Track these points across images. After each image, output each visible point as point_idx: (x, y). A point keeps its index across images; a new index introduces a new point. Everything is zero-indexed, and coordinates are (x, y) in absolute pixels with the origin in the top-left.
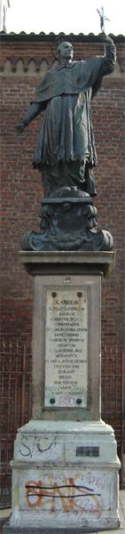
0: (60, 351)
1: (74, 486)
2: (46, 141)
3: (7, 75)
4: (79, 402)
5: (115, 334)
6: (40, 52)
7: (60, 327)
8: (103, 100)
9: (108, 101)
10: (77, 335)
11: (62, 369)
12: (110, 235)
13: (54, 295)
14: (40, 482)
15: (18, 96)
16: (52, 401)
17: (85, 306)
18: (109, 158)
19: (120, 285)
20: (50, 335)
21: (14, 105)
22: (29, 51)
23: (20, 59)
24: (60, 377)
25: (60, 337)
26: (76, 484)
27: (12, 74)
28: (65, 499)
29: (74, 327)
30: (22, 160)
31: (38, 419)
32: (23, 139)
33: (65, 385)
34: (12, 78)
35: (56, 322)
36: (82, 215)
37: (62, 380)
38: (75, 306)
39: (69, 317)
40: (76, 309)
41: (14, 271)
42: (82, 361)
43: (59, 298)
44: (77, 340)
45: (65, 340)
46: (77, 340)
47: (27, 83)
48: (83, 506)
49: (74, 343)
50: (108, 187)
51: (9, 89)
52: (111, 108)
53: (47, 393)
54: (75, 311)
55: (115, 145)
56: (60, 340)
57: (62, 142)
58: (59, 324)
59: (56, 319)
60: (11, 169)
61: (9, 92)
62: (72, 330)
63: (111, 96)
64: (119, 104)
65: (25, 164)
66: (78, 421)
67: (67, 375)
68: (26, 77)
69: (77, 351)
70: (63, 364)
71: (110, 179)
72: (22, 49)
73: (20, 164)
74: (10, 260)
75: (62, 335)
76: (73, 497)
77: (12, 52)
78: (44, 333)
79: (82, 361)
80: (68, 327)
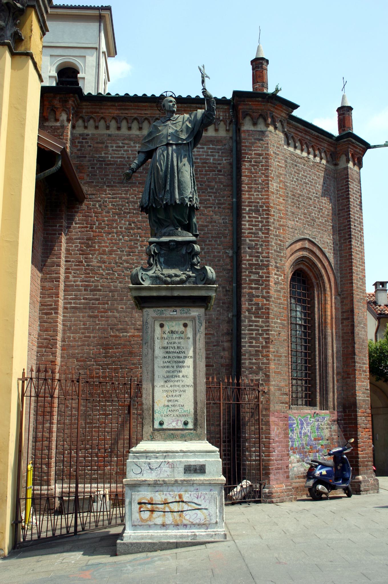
0: (167, 377)
1: (183, 502)
2: (152, 186)
3: (113, 133)
4: (186, 423)
5: (212, 366)
6: (143, 112)
7: (167, 355)
8: (200, 155)
9: (204, 157)
11: (171, 394)
12: (213, 270)
13: (162, 326)
14: (151, 499)
15: (122, 152)
16: (161, 424)
17: (190, 335)
18: (205, 207)
19: (216, 322)
20: (159, 363)
21: (119, 160)
22: (133, 111)
23: (125, 118)
25: (168, 364)
26: (185, 500)
27: (117, 132)
28: (175, 514)
29: (180, 355)
30: (127, 209)
31: (148, 440)
33: (173, 408)
34: (117, 136)
35: (164, 350)
36: (186, 252)
39: (176, 345)
40: (182, 338)
43: (166, 328)
45: (173, 367)
47: (131, 140)
48: (191, 520)
50: (204, 234)
51: (114, 145)
52: (206, 163)
53: (156, 416)
54: (181, 340)
55: (211, 196)
56: (168, 367)
57: (168, 188)
58: (167, 352)
59: (164, 348)
60: (117, 217)
61: (114, 148)
62: (178, 357)
63: (208, 152)
64: (214, 159)
65: (129, 213)
66: (186, 441)
67: (176, 398)
68: (130, 135)
69: (183, 376)
70: (171, 389)
71: (207, 226)
72: (128, 109)
73: (125, 213)
74: (116, 300)
76: (182, 511)
77: (117, 112)
78: (153, 360)
80: (176, 355)
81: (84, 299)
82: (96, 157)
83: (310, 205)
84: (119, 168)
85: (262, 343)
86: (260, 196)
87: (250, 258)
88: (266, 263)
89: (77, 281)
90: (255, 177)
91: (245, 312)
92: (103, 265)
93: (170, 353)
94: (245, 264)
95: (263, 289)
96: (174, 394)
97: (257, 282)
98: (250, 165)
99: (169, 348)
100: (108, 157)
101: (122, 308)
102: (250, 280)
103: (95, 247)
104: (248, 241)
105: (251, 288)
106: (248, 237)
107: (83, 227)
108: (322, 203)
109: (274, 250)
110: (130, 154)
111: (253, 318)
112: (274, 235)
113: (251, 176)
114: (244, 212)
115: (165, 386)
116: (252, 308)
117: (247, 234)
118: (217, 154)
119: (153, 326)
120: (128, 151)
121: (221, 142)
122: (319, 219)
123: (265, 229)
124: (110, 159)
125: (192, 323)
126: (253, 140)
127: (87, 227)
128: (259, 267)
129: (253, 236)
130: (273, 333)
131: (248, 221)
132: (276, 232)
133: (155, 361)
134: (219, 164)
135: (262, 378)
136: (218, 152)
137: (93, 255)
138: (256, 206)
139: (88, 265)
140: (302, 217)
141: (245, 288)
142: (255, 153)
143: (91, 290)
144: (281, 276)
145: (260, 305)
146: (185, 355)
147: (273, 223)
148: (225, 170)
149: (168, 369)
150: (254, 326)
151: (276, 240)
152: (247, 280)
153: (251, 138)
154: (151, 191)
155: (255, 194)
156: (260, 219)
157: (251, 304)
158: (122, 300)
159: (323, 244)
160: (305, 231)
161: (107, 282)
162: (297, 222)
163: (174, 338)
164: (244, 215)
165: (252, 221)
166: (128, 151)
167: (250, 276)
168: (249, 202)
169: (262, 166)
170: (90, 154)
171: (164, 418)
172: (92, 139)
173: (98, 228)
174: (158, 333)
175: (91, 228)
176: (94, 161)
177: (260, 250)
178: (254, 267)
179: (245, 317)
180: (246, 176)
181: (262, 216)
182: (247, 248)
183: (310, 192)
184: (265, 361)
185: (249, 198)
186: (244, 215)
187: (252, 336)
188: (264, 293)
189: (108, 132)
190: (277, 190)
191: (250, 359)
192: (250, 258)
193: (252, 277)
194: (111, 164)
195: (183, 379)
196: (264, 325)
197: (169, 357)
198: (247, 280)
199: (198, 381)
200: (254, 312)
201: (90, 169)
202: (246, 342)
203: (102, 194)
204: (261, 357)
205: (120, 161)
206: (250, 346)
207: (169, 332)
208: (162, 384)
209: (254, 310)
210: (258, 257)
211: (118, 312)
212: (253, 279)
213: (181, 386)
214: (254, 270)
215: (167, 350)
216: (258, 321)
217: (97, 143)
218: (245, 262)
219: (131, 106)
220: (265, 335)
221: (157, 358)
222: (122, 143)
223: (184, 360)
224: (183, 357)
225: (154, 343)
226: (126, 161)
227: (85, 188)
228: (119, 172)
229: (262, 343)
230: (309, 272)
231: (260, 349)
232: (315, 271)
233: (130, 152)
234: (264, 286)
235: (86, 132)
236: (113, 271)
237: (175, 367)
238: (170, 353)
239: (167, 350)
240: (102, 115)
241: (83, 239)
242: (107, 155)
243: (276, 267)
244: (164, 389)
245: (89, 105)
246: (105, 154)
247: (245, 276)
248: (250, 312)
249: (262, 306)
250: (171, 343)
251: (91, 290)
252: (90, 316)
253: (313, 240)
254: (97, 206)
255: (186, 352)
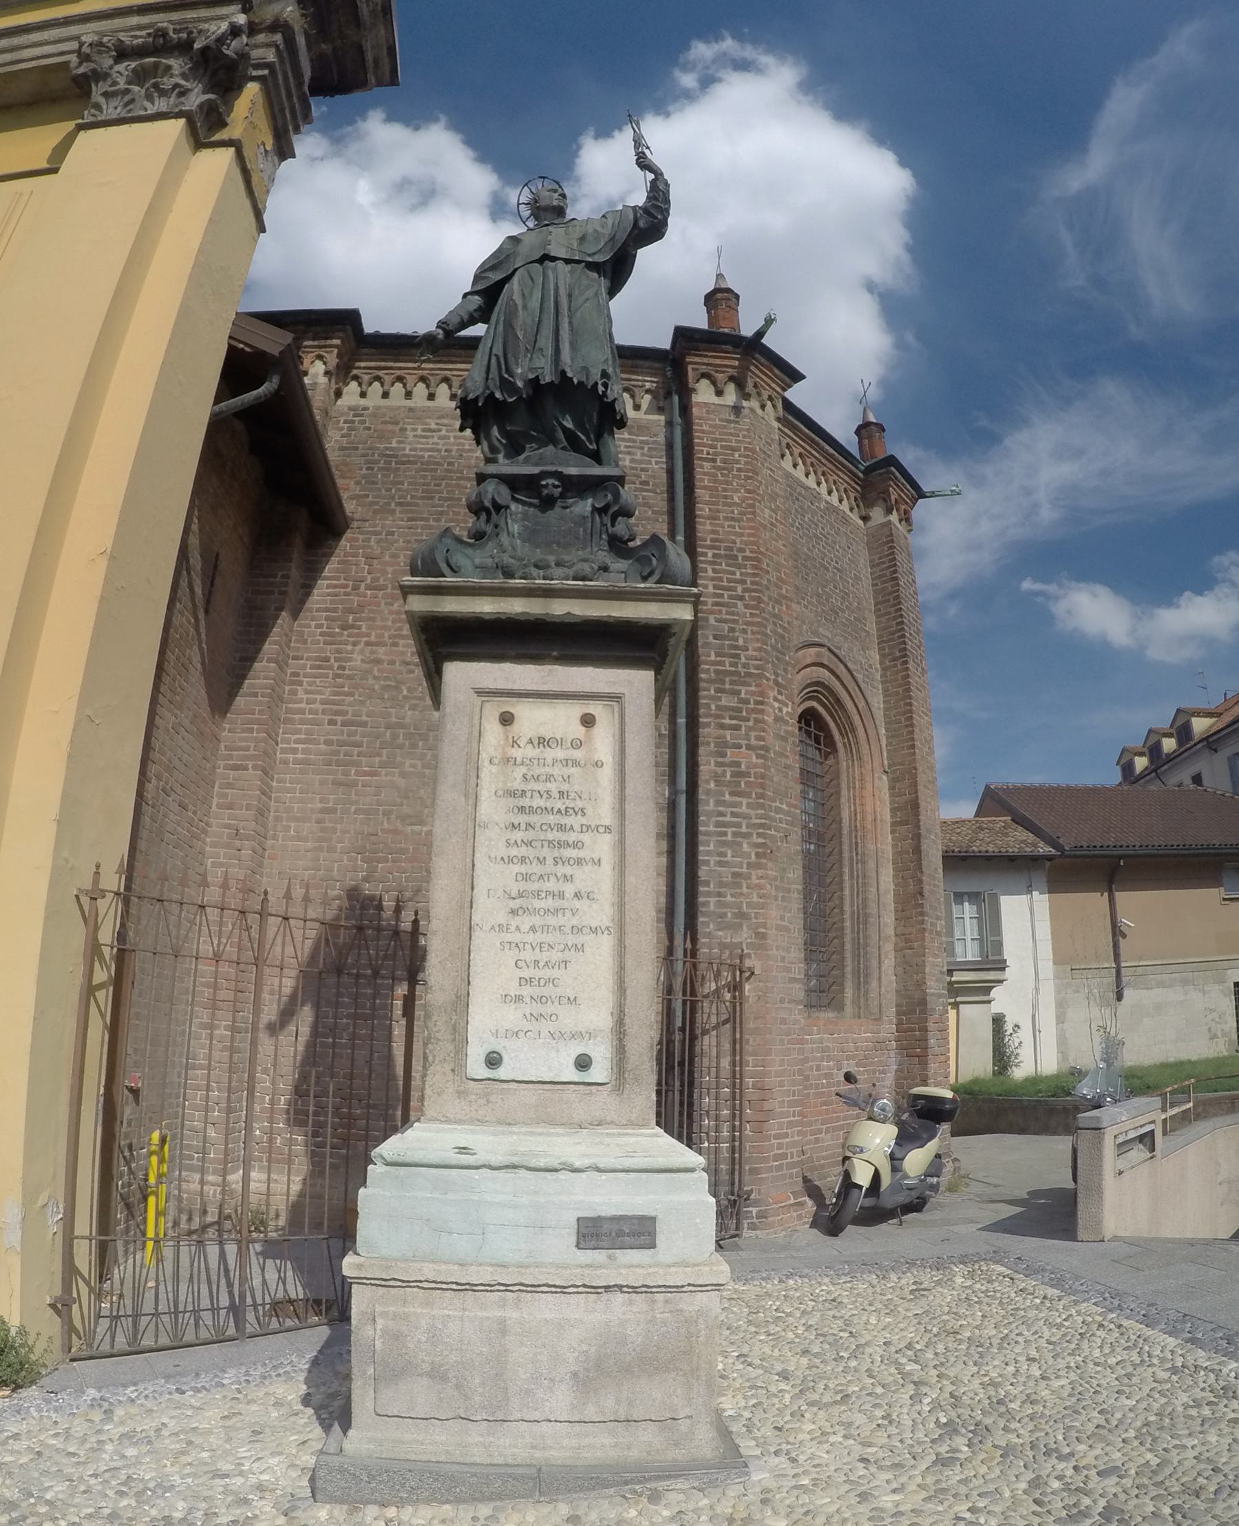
4: (583, 1063)
7: (522, 819)
10: (577, 845)
11: (528, 955)
13: (507, 719)
16: (493, 1061)
20: (492, 843)
21: (427, 454)
24: (523, 981)
25: (523, 851)
29: (567, 821)
32: (442, 513)
34: (426, 410)
35: (511, 802)
37: (526, 991)
38: (577, 754)
39: (552, 786)
40: (576, 763)
41: (407, 769)
42: (594, 931)
44: (579, 862)
45: (542, 861)
46: (579, 862)
49: (568, 870)
51: (420, 427)
56: (523, 860)
58: (522, 809)
59: (512, 794)
61: (419, 432)
62: (561, 828)
64: (632, 461)
67: (548, 973)
69: (577, 895)
74: (401, 747)
75: (529, 844)
79: (594, 931)
80: (551, 819)
81: (326, 742)
82: (378, 449)
83: (827, 581)
84: (425, 470)
85: (748, 855)
86: (737, 529)
87: (718, 659)
88: (756, 672)
89: (314, 701)
90: (725, 490)
91: (708, 782)
92: (376, 669)
93: (532, 811)
94: (708, 671)
95: (749, 729)
96: (543, 957)
97: (735, 712)
98: (714, 467)
99: (529, 794)
100: (404, 449)
101: (414, 766)
102: (718, 708)
103: (359, 628)
104: (712, 621)
105: (722, 727)
106: (712, 613)
107: (336, 586)
108: (848, 582)
109: (771, 645)
110: (453, 444)
111: (727, 796)
112: (770, 613)
113: (717, 488)
114: (702, 559)
115: (513, 929)
116: (724, 771)
117: (709, 607)
118: (639, 452)
119: (476, 721)
120: (449, 438)
121: (648, 429)
122: (843, 611)
123: (752, 598)
124: (407, 452)
125: (610, 716)
126: (718, 422)
127: (346, 586)
128: (740, 679)
129: (724, 610)
130: (773, 833)
131: (713, 579)
132: (773, 608)
133: (480, 838)
134: (642, 470)
135: (749, 940)
136: (642, 448)
137: (355, 644)
138: (731, 549)
139: (339, 668)
140: (814, 601)
141: (708, 724)
142: (721, 446)
143: (344, 724)
144: (787, 705)
145: (743, 766)
146: (584, 821)
147: (768, 589)
148: (657, 481)
149: (523, 869)
150: (729, 815)
151: (775, 624)
152: (713, 707)
153: (712, 416)
154: (494, 360)
155: (727, 523)
156: (738, 576)
157: (721, 763)
158: (414, 746)
159: (855, 663)
160: (821, 630)
161: (383, 705)
162: (806, 607)
163: (549, 761)
164: (703, 565)
165: (721, 579)
166: (449, 438)
167: (720, 699)
168: (712, 540)
169: (739, 470)
170: (366, 443)
171: (505, 1042)
172: (374, 415)
173: (368, 588)
174: (494, 742)
175: (356, 588)
176: (373, 455)
177: (741, 642)
178: (727, 679)
179: (708, 792)
180: (705, 488)
181: (743, 571)
182: (711, 638)
183: (825, 555)
184: (755, 899)
185: (713, 532)
186: (703, 565)
187: (723, 838)
188: (753, 739)
189: (408, 403)
190: (772, 524)
191: (719, 894)
192: (718, 659)
193: (724, 702)
194: (409, 462)
195: (577, 904)
196: (752, 813)
197: (529, 826)
198: (713, 707)
199: (630, 915)
200: (730, 782)
201: (364, 471)
202: (709, 852)
203: (386, 519)
204: (745, 890)
205: (429, 456)
206: (720, 864)
207: (531, 741)
208: (502, 918)
209: (728, 777)
210: (737, 656)
211: (403, 775)
212: (726, 706)
213: (568, 930)
214: (727, 686)
215: (521, 802)
216: (739, 805)
217: (385, 423)
218: (707, 667)
219: (460, 356)
220: (755, 836)
221: (486, 826)
222: (437, 424)
223: (581, 836)
224: (577, 828)
225: (478, 777)
226: (442, 457)
227: (349, 507)
228: (424, 477)
229: (748, 855)
230: (828, 719)
231: (745, 870)
232: (840, 718)
233: (452, 440)
234: (751, 724)
235: (363, 402)
236: (397, 682)
237: (550, 861)
238: (532, 811)
239: (521, 802)
240: (399, 373)
241: (335, 610)
242: (402, 445)
243: (777, 683)
244: (508, 937)
245: (373, 355)
246: (399, 442)
247: (707, 697)
248: (718, 783)
249: (748, 767)
250: (537, 779)
251: (344, 724)
252: (337, 783)
253: (837, 651)
254: (372, 543)
255: (589, 811)
